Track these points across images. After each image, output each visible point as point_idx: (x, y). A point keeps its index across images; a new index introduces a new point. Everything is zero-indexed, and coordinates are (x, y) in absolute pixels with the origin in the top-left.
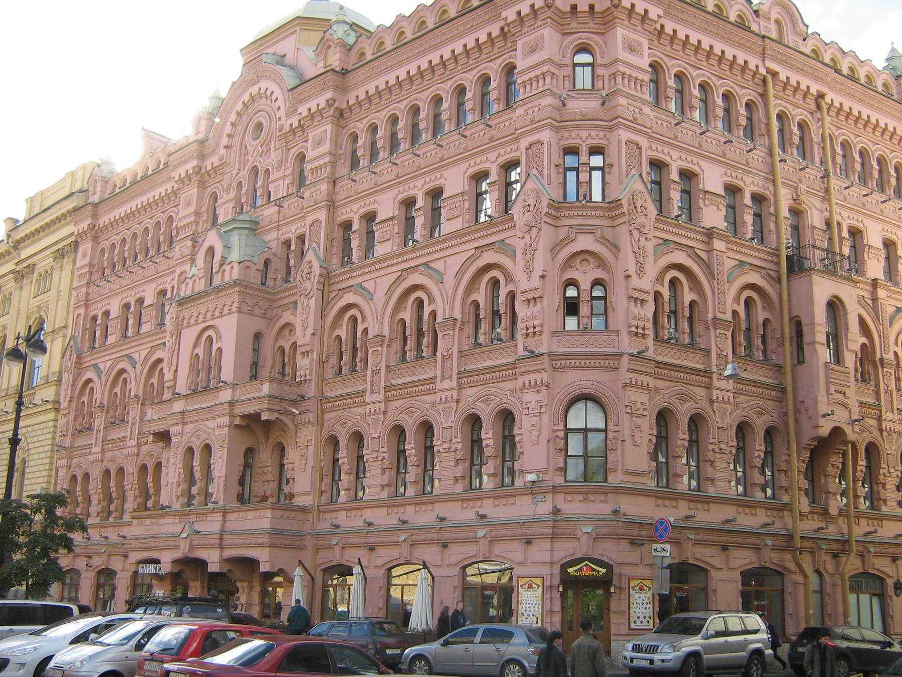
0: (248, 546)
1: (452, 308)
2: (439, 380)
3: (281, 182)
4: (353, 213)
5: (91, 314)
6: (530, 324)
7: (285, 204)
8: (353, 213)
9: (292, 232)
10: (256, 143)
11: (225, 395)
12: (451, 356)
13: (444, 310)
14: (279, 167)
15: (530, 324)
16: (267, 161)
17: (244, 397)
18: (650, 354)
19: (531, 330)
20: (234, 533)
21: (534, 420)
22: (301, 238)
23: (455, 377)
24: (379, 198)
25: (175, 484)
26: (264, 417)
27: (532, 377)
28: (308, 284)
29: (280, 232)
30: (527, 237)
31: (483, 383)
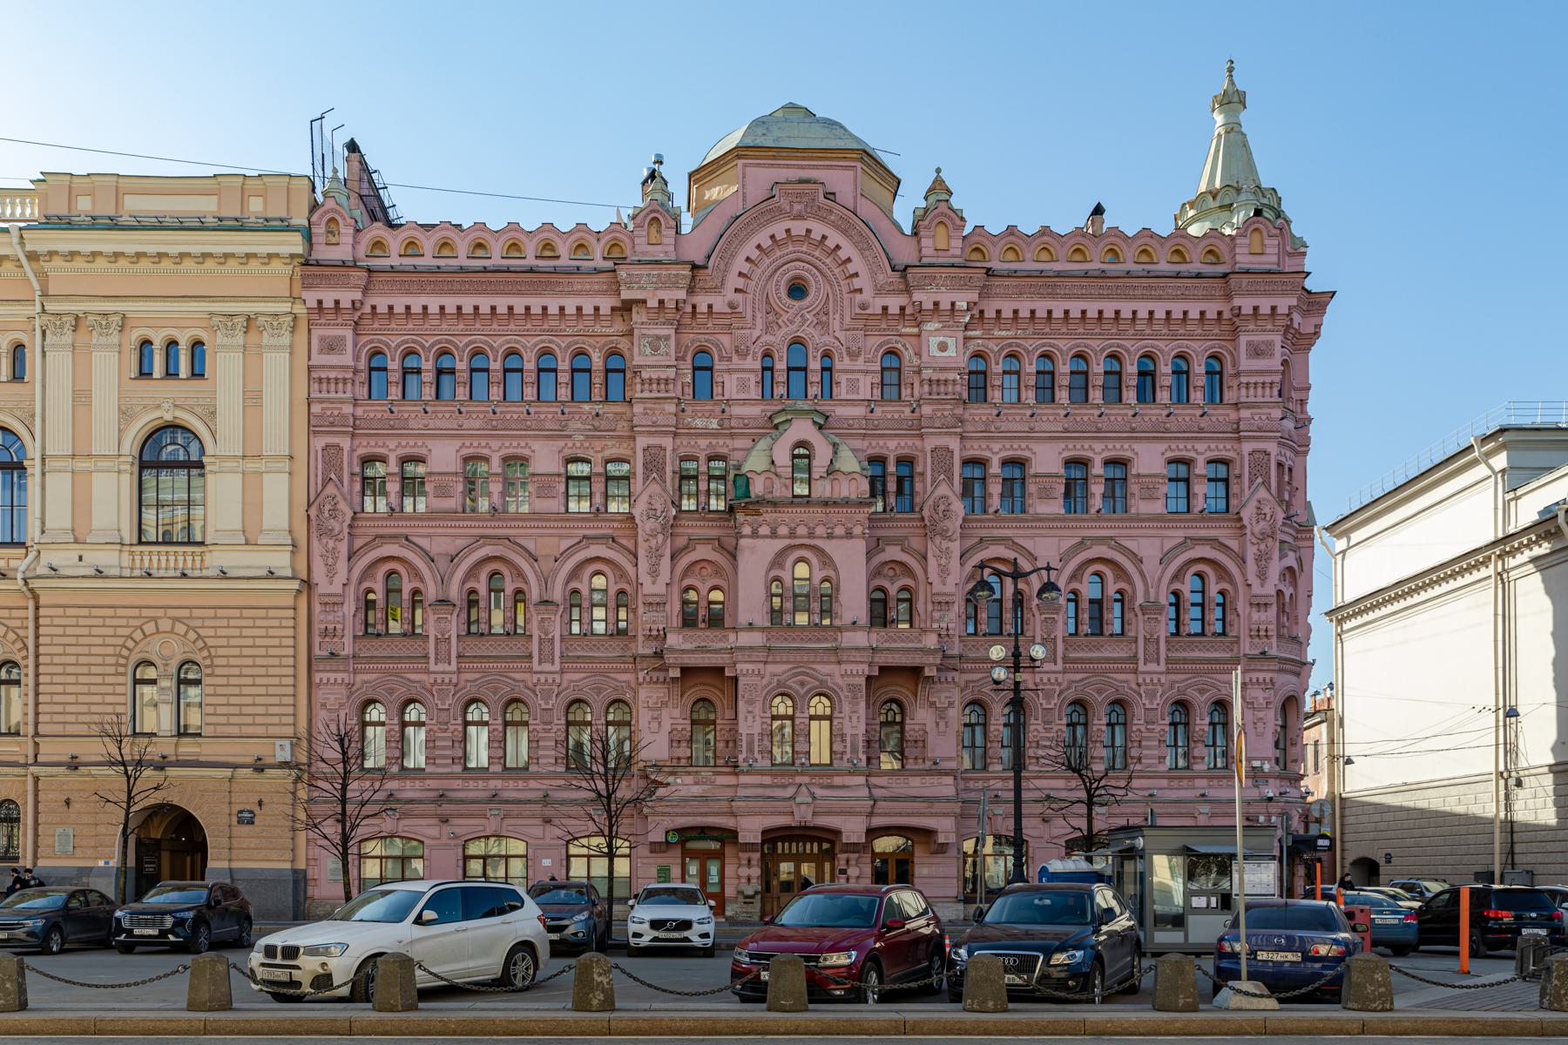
0: (908, 815)
1: (1157, 594)
2: (1141, 661)
3: (860, 376)
4: (995, 454)
5: (361, 451)
6: (1263, 627)
7: (878, 411)
8: (995, 454)
9: (892, 447)
10: (797, 304)
11: (860, 639)
12: (1158, 641)
13: (1147, 592)
14: (853, 355)
15: (1263, 627)
16: (826, 339)
17: (887, 645)
18: (1273, 652)
19: (1262, 633)
20: (885, 799)
21: (1261, 714)
22: (906, 461)
23: (1162, 661)
24: (1035, 446)
25: (756, 738)
26: (927, 673)
27: (1261, 676)
28: (947, 523)
29: (866, 443)
30: (1263, 547)
31: (1197, 673)
